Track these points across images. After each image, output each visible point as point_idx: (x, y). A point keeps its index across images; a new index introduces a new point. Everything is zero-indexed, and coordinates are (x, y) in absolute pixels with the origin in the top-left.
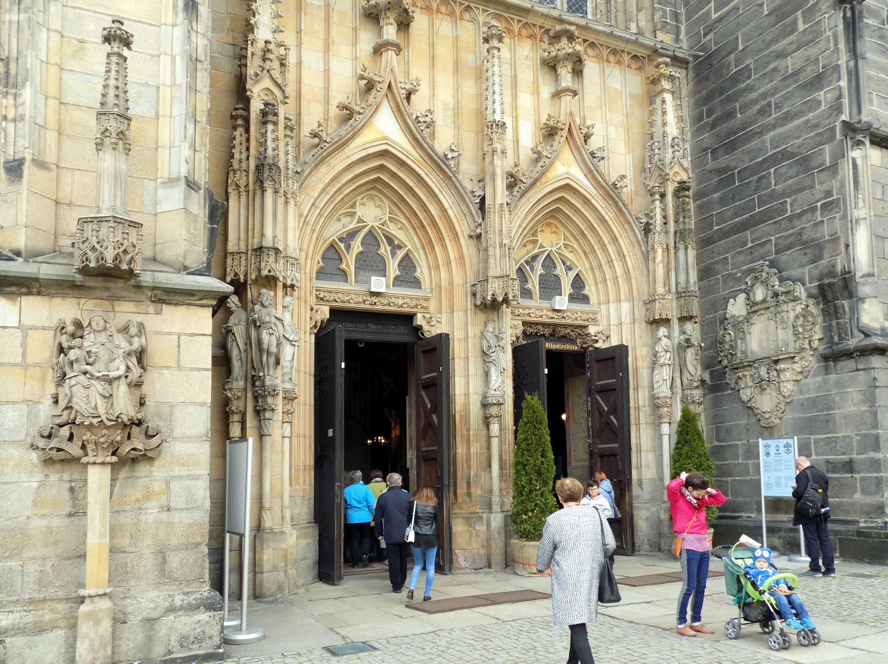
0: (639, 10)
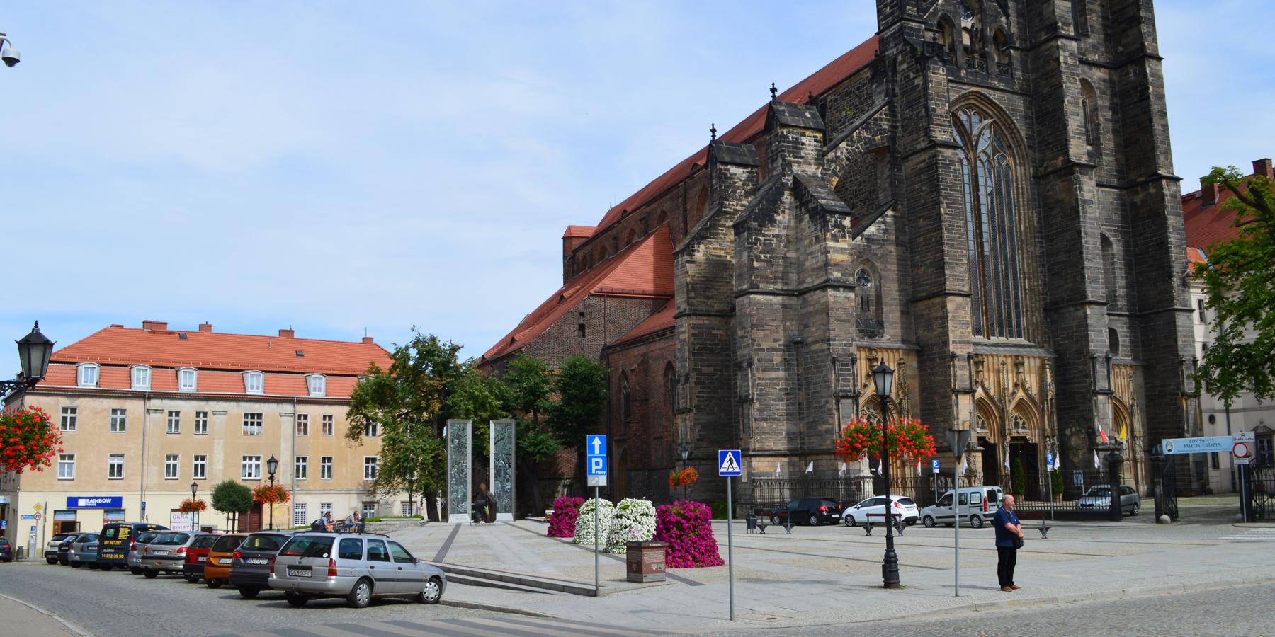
0: (1038, 334)
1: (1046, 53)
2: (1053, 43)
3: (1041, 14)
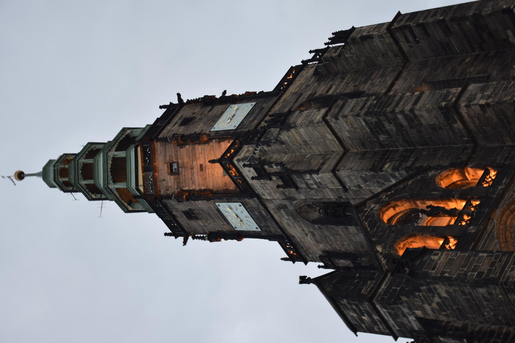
1: (477, 122)
2: (464, 111)
3: (433, 127)
